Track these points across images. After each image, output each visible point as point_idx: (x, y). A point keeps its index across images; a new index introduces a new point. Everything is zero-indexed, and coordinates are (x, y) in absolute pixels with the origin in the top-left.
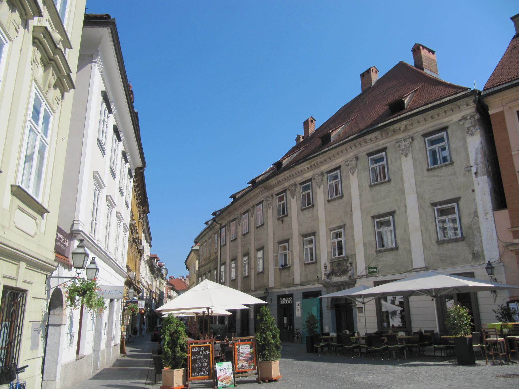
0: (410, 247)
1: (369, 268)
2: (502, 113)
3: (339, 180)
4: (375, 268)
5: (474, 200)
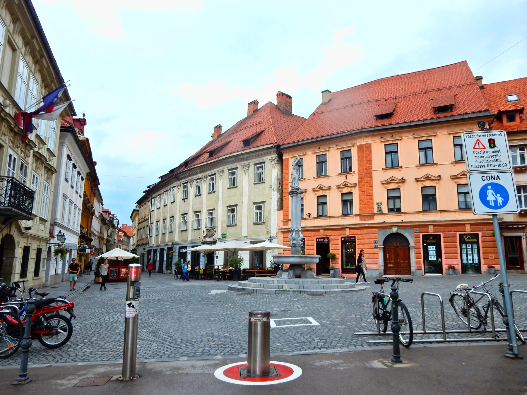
0: (242, 224)
1: (223, 235)
2: (288, 159)
3: (214, 182)
4: (226, 235)
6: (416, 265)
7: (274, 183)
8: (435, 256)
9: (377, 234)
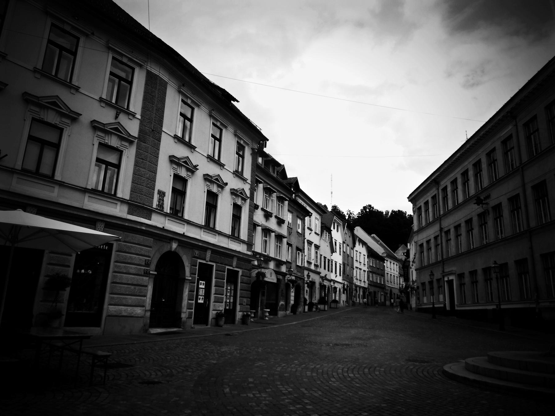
6: (188, 310)
8: (203, 297)
9: (151, 247)
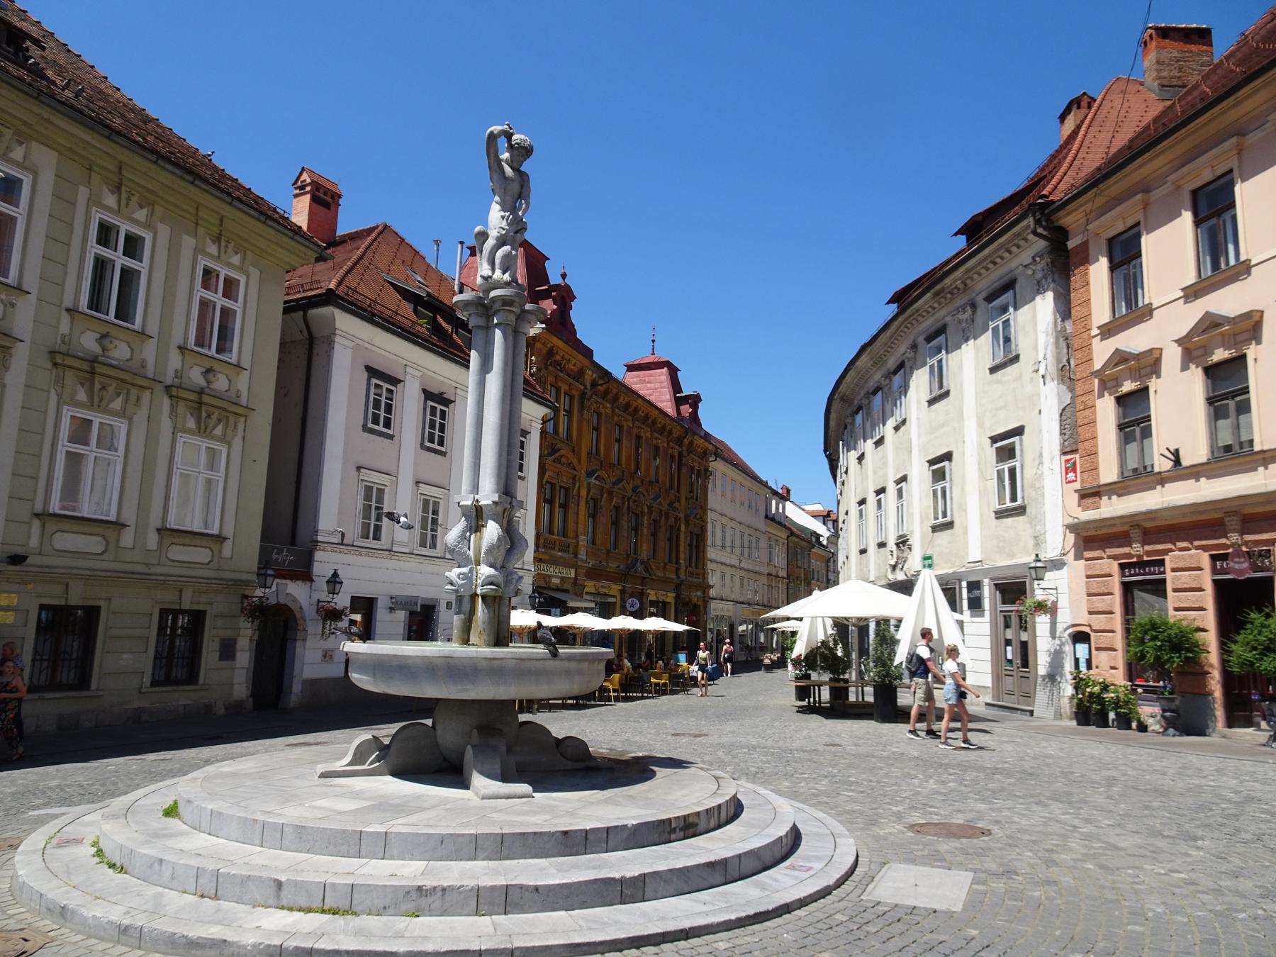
5: (1041, 430)
7: (1046, 349)
